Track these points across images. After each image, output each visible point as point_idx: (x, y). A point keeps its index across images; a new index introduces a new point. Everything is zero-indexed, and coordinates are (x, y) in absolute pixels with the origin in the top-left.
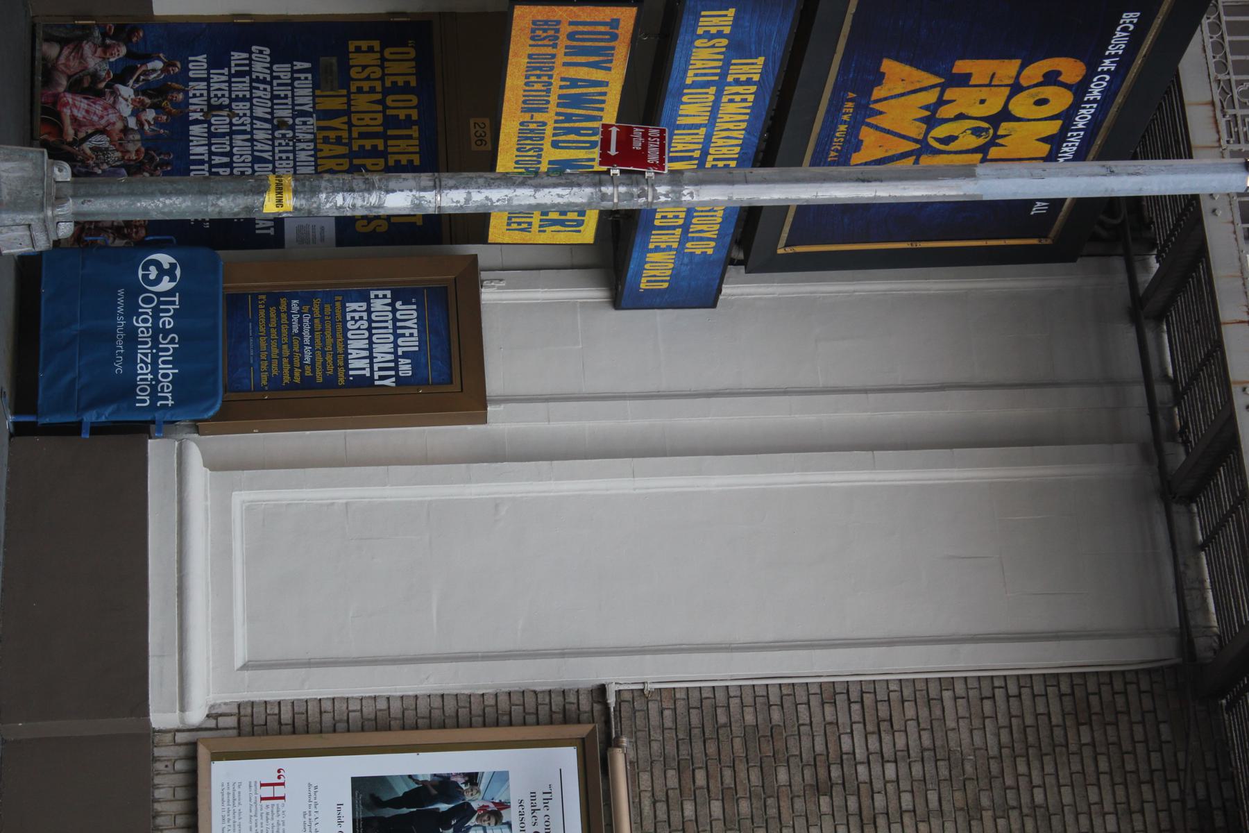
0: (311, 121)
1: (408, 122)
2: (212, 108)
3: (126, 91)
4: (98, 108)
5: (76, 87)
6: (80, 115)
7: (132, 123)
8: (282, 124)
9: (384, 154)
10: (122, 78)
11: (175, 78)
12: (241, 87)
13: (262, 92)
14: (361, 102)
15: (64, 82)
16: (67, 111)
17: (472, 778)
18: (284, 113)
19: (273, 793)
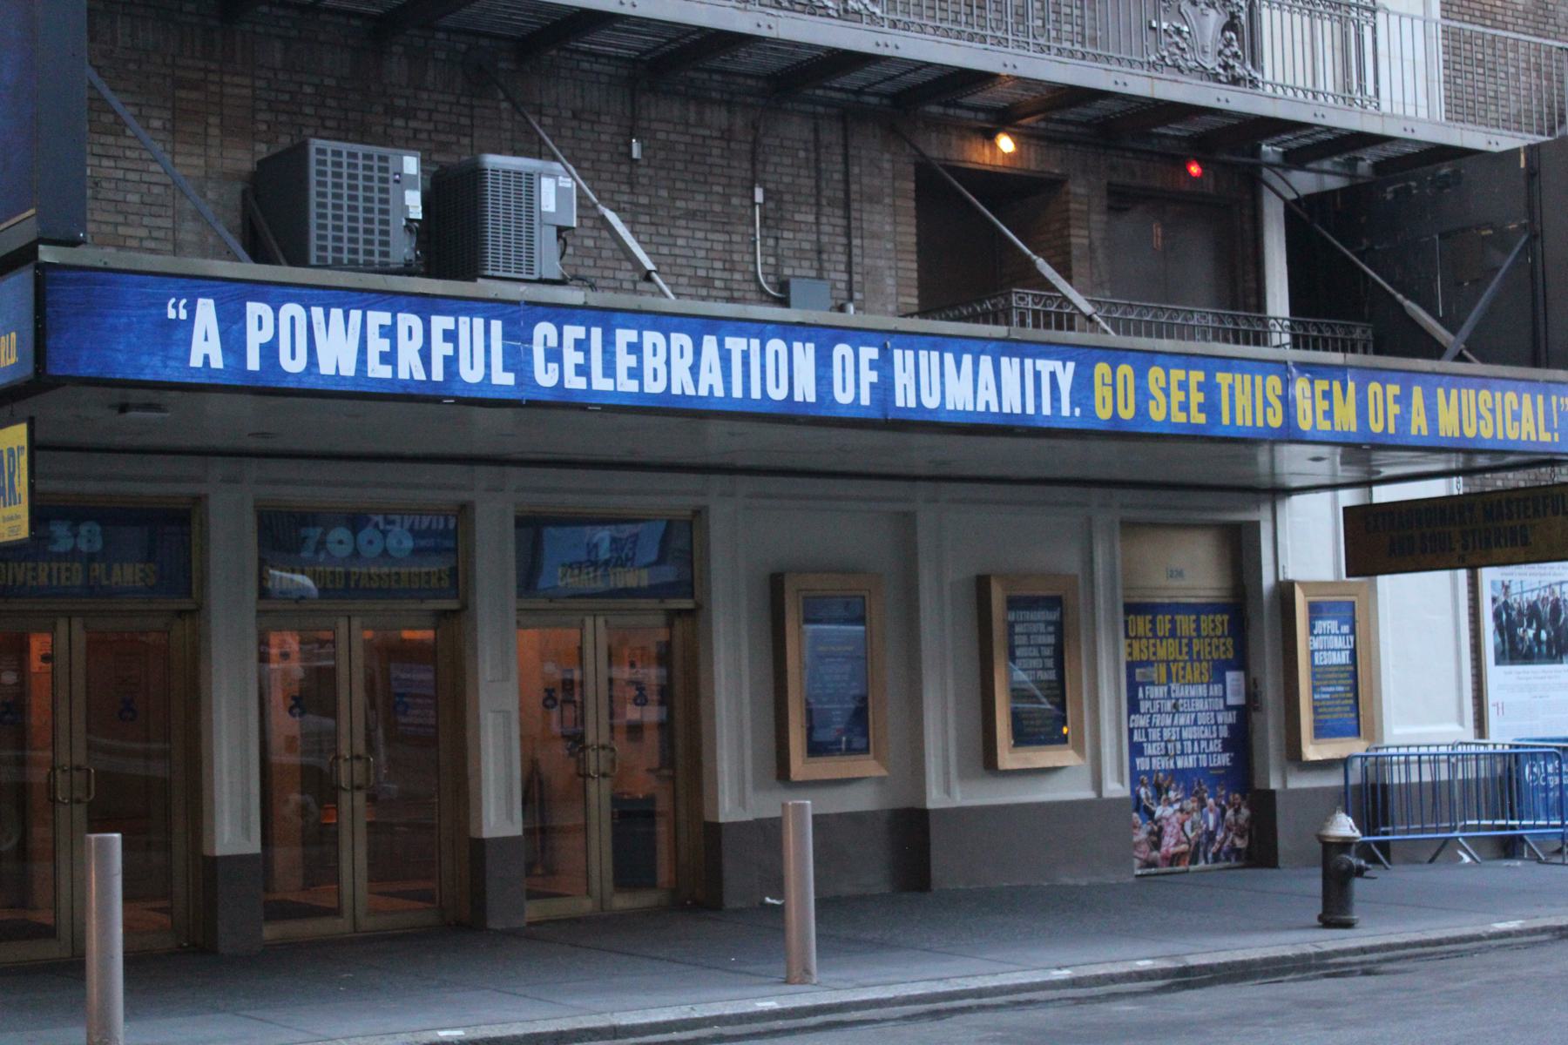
0: (1173, 686)
1: (1173, 621)
2: (1166, 754)
3: (1159, 811)
4: (1169, 829)
5: (1157, 845)
6: (1173, 841)
7: (1177, 806)
8: (1175, 706)
9: (1191, 639)
10: (1151, 814)
11: (1150, 778)
12: (1154, 734)
13: (1157, 720)
14: (1162, 653)
15: (1155, 854)
16: (1172, 850)
17: (1494, 600)
18: (1169, 705)
19: (1501, 708)
